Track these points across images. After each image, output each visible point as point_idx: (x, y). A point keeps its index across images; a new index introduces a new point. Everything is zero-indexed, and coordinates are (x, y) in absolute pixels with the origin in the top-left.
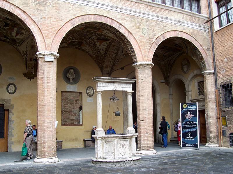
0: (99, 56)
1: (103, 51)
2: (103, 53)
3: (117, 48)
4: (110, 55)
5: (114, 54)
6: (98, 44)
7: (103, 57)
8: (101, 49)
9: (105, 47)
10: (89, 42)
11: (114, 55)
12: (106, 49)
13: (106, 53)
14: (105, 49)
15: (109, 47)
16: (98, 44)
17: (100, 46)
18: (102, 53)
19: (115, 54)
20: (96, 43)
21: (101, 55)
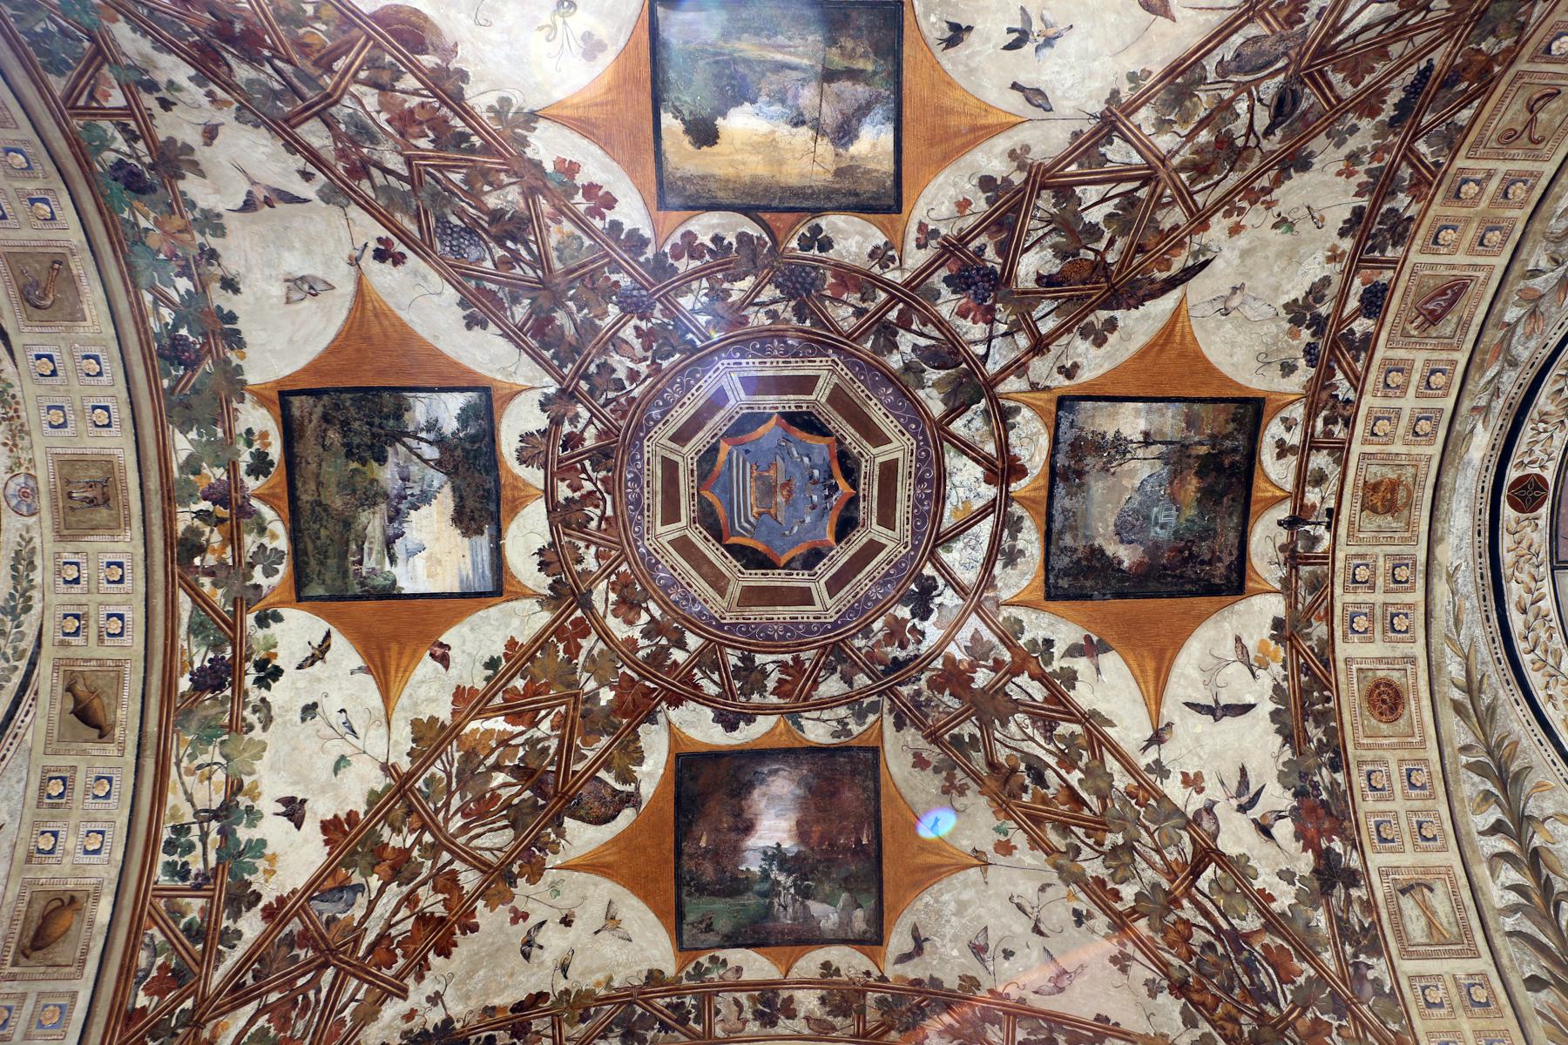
0: (1250, 968)
1: (1265, 830)
2: (1287, 876)
3: (1459, 732)
4: (1440, 902)
5: (1481, 871)
6: (1108, 689)
7: (1327, 956)
8: (1212, 790)
9: (1257, 745)
10: (954, 678)
11: (1497, 895)
12: (1298, 779)
13: (1331, 875)
14: (1277, 797)
15: (1316, 733)
16: (1108, 689)
17: (1157, 738)
18: (1265, 880)
19: (1510, 875)
20: (1070, 677)
21: (1273, 923)
